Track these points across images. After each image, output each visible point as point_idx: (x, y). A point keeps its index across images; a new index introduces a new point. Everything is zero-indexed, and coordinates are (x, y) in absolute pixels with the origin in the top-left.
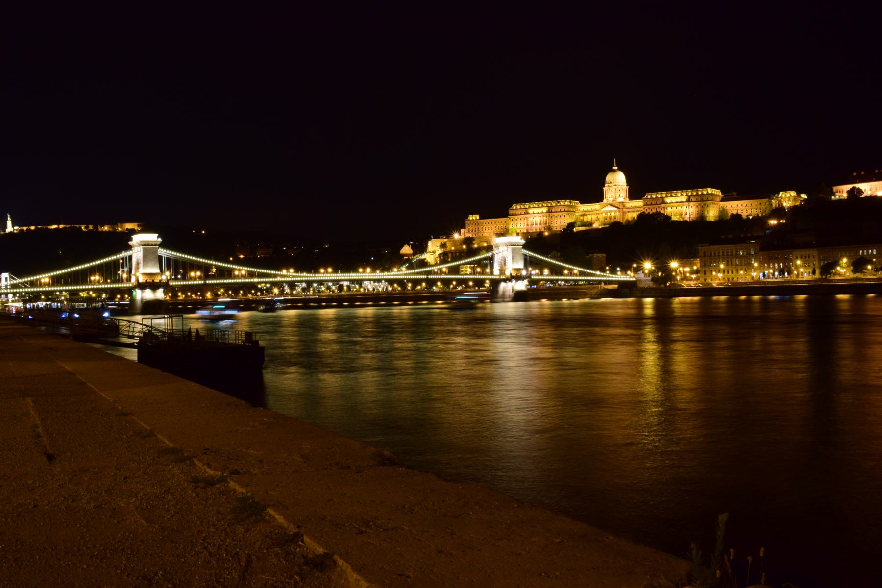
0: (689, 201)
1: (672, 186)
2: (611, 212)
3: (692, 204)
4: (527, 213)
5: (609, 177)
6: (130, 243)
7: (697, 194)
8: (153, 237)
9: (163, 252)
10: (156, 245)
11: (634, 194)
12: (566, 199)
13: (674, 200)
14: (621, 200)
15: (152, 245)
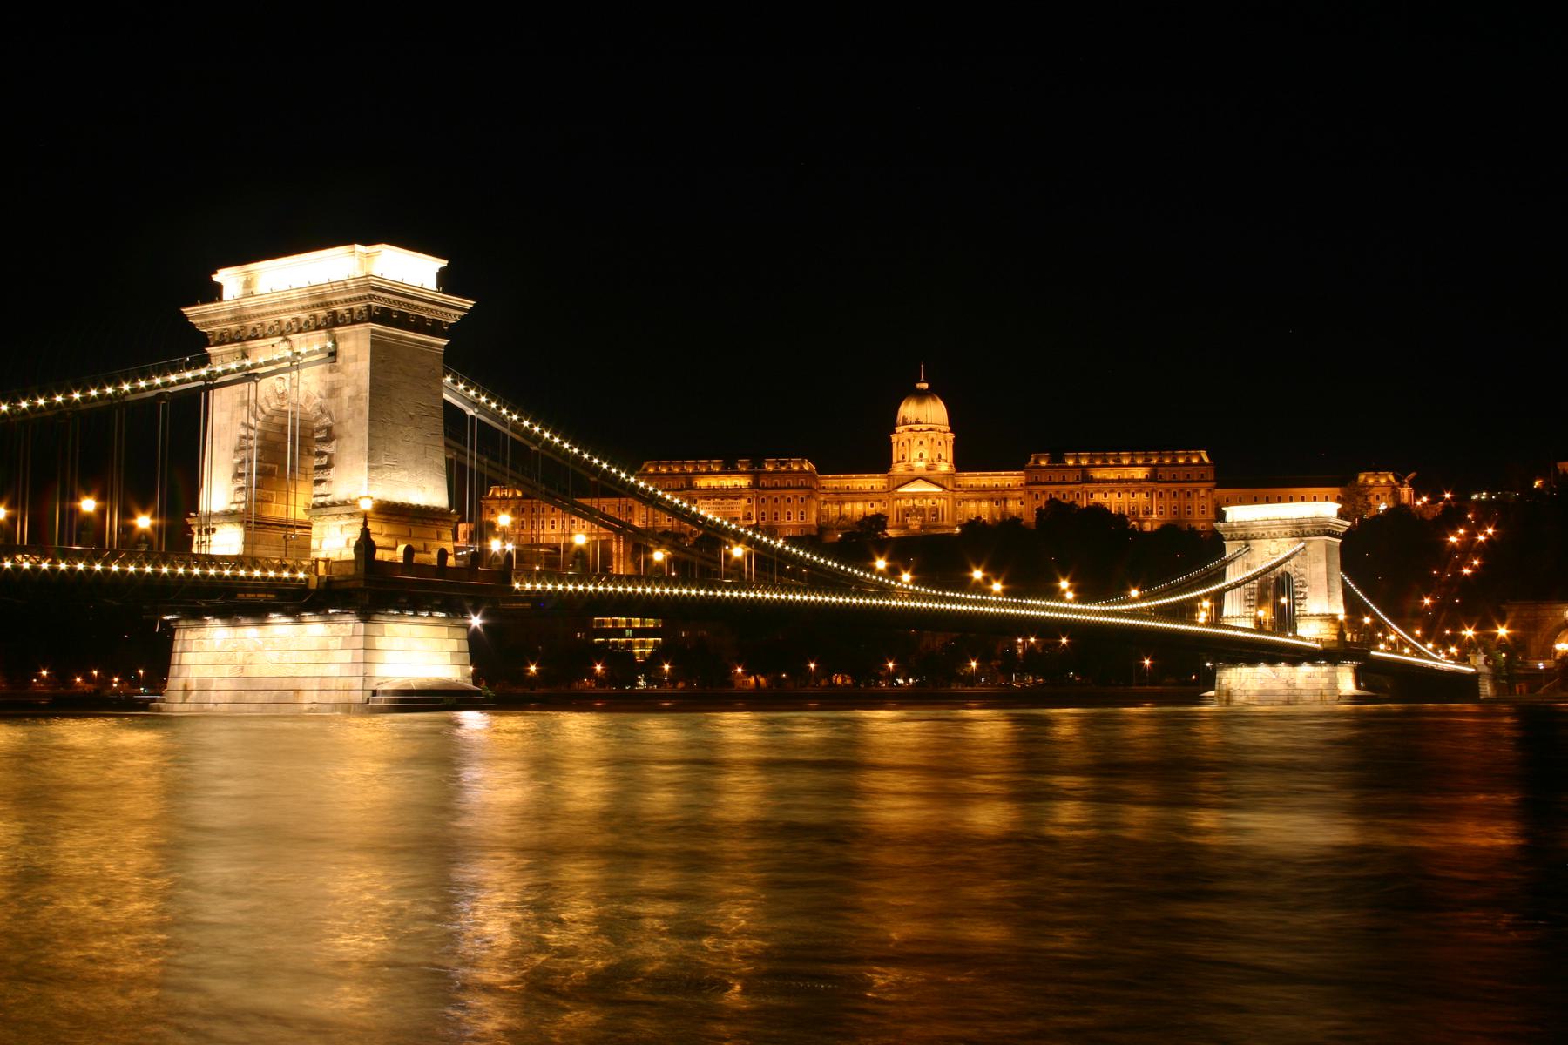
0: (1153, 478)
1: (1108, 443)
2: (926, 496)
3: (1161, 487)
4: (691, 487)
5: (908, 410)
6: (196, 313)
7: (1174, 464)
8: (413, 270)
9: (456, 392)
10: (435, 328)
11: (971, 453)
12: (804, 455)
13: (1112, 474)
14: (944, 468)
15: (420, 325)
